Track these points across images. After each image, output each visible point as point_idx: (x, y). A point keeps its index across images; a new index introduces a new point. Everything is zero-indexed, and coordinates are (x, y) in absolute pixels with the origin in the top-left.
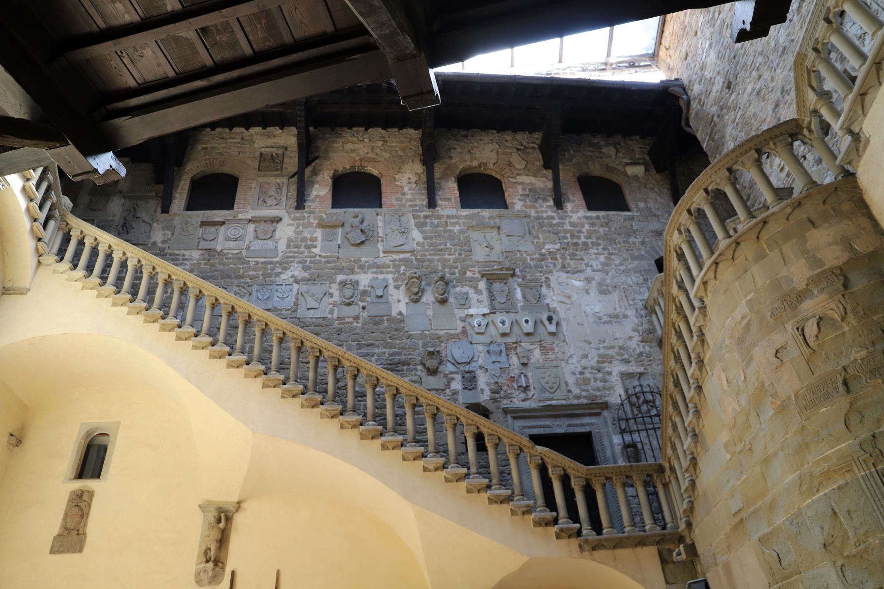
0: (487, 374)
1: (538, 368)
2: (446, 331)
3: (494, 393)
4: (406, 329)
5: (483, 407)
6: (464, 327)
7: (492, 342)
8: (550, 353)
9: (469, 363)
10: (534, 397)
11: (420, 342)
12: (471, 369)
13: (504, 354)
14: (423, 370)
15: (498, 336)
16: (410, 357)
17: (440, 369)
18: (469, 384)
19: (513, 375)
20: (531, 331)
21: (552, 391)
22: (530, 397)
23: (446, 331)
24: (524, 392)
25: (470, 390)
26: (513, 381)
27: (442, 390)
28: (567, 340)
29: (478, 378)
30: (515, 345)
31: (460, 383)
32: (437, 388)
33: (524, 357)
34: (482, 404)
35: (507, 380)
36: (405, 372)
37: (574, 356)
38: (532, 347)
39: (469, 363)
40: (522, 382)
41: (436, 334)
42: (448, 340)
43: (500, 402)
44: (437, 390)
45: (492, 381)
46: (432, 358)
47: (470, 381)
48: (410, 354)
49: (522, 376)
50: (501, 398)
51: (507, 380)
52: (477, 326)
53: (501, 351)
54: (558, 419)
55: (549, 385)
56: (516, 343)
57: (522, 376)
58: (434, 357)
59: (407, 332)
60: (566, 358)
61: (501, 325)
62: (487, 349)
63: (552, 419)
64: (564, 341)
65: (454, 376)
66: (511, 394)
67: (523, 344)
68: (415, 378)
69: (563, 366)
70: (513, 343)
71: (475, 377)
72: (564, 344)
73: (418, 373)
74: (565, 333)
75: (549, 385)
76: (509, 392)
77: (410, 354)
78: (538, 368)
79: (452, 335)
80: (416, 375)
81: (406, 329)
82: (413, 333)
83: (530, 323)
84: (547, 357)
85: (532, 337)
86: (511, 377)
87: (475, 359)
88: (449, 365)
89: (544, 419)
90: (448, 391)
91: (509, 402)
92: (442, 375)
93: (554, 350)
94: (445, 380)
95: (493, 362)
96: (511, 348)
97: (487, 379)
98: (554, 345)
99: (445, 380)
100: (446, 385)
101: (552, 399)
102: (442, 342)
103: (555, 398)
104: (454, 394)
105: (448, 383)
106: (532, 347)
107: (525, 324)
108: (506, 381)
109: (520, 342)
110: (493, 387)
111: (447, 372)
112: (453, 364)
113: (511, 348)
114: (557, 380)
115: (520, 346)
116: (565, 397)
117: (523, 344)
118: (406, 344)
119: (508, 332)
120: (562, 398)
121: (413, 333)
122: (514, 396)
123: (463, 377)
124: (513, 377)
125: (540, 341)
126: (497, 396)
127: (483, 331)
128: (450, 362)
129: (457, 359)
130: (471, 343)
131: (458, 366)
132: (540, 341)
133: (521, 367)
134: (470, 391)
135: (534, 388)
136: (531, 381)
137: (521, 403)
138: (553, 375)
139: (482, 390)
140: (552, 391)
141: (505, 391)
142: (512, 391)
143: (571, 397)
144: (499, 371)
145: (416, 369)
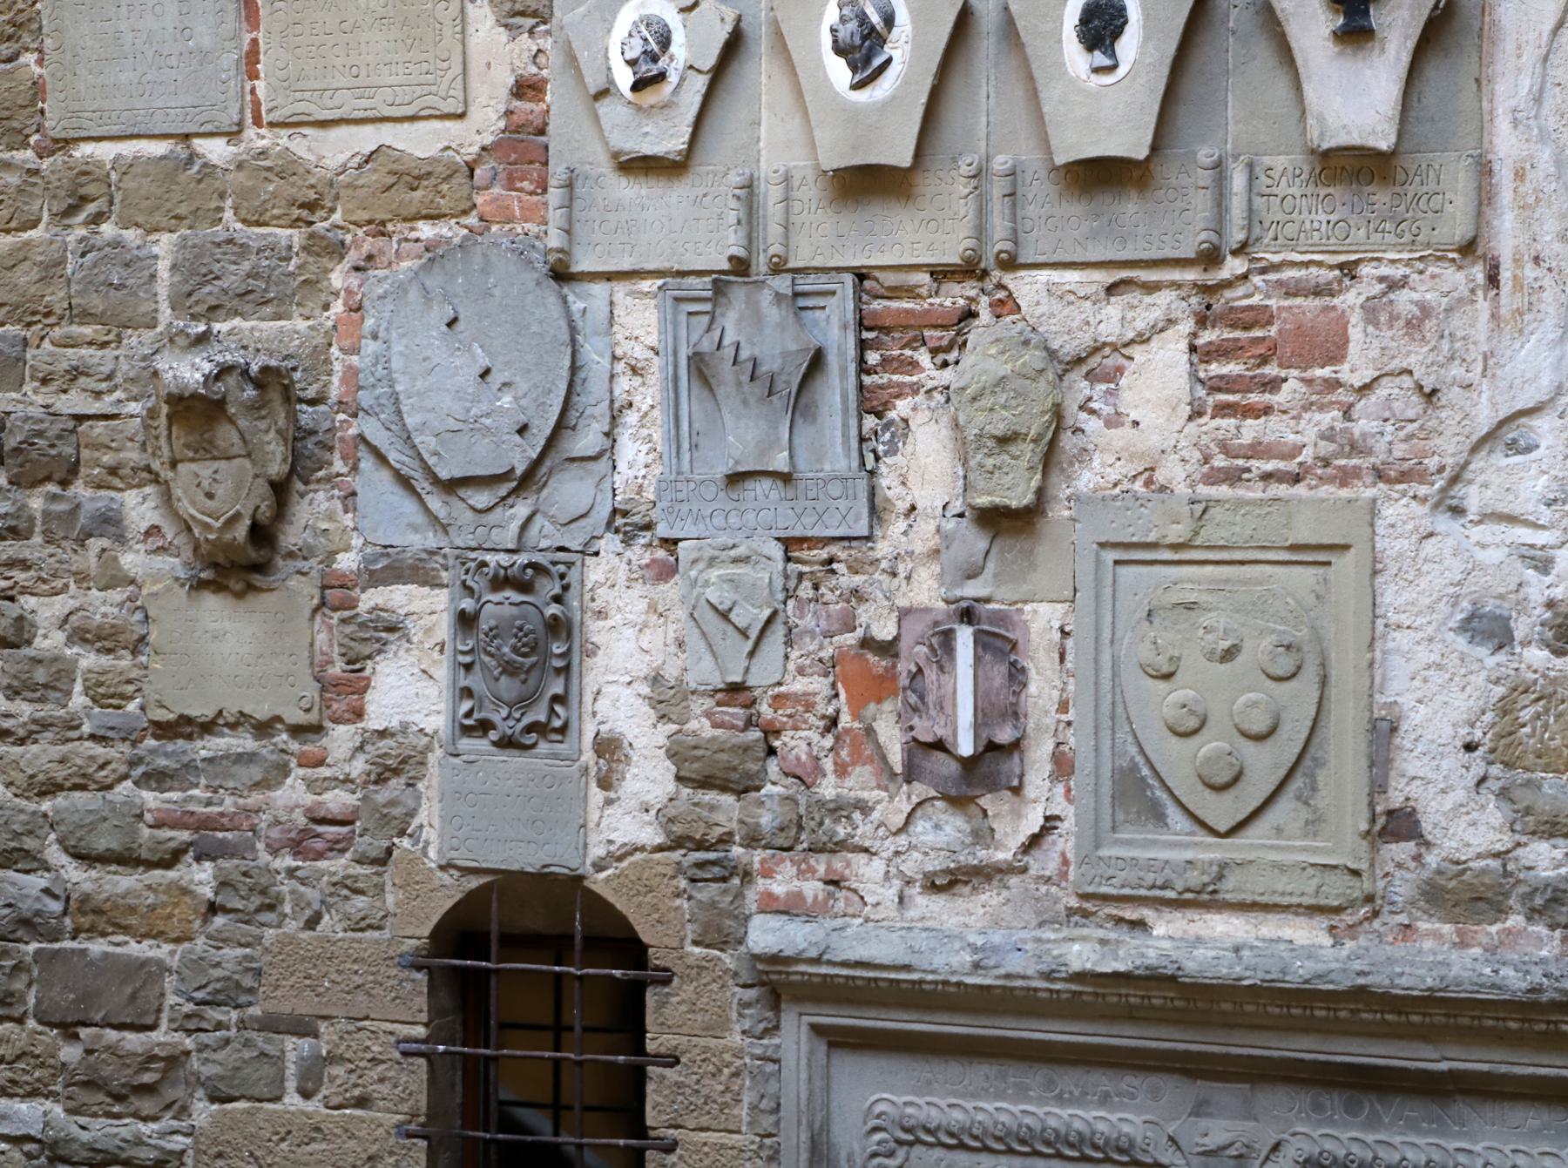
0: (671, 590)
1: (1131, 552)
2: (367, 139)
3: (705, 783)
4: (55, 124)
5: (597, 904)
6: (526, 88)
7: (741, 266)
8: (1292, 390)
9: (527, 480)
10: (1045, 862)
11: (164, 245)
12: (545, 534)
13: (836, 389)
14: (169, 531)
15: (810, 193)
16: (74, 402)
17: (291, 537)
18: (508, 687)
19: (885, 630)
20: (1131, 142)
21: (1222, 811)
22: (1002, 856)
23: (367, 139)
24: (958, 802)
25: (507, 743)
26: (882, 687)
27: (297, 731)
28: (1506, 236)
29: (596, 631)
30: (954, 296)
31: (442, 672)
32: (262, 712)
33: (1004, 441)
34: (599, 882)
35: (830, 666)
36: (34, 548)
37: (1544, 428)
38: (1112, 320)
39: (527, 480)
40: (946, 706)
41: (288, 169)
42: (380, 230)
43: (747, 876)
44: (263, 729)
45: (706, 673)
46: (206, 450)
47: (510, 669)
48: (76, 373)
49: (965, 637)
50: (753, 840)
51: (830, 666)
52: (624, 78)
53: (817, 361)
54: (1226, 1094)
55: (1208, 746)
56: (970, 270)
57: (965, 637)
58: (226, 436)
59: (65, 143)
60: (1448, 448)
61: (839, 72)
62: (695, 336)
63: (1173, 1089)
64: (1468, 249)
65: (399, 597)
66: (838, 809)
67: (1028, 287)
68: (104, 606)
69: (1392, 546)
70: (941, 274)
71: (558, 627)
72: (1459, 279)
73: (132, 560)
74: (1506, 143)
75: (1208, 746)
76: (828, 788)
77: (76, 373)
78: (1131, 552)
79: (411, 176)
80: (115, 579)
81: (55, 124)
82: (106, 151)
83: (1129, 45)
84: (1251, 430)
85: (1130, 208)
86: (867, 643)
87: (587, 440)
88: (374, 484)
89: (1102, 1080)
90: (341, 737)
91: (812, 889)
92: (305, 591)
93: (1335, 352)
94: (325, 636)
95: (736, 479)
96: (914, 330)
97: (656, 638)
98: (1351, 298)
99: (325, 636)
100: (327, 686)
101: (1204, 899)
102: (338, 250)
103: (1231, 888)
104: (383, 774)
105: (355, 662)
106: (1112, 320)
107: (1076, 59)
108: (818, 685)
109: (1010, 264)
110: (700, 726)
111: (347, 562)
112: (405, 482)
113: (914, 330)
114: (1299, 699)
115: (1006, 305)
116: (1336, 889)
117: (1028, 287)
118: (52, 269)
119: (902, 156)
120: (1304, 888)
121: (106, 151)
122: (864, 831)
123: (466, 621)
124: (888, 649)
125: (1210, 258)
126: (727, 809)
127: (669, 140)
128: (381, 458)
129: (425, 442)
130: (561, 275)
131: (435, 503)
132: (1210, 258)
133: (976, 541)
134: (514, 760)
135: (1062, 766)
136: (1042, 688)
137: (925, 905)
138: (1258, 649)
139: (608, 747)
140: (1222, 811)
141: (803, 778)
142: (860, 783)
143: (1403, 887)
144: (770, 568)
145: (110, 523)
